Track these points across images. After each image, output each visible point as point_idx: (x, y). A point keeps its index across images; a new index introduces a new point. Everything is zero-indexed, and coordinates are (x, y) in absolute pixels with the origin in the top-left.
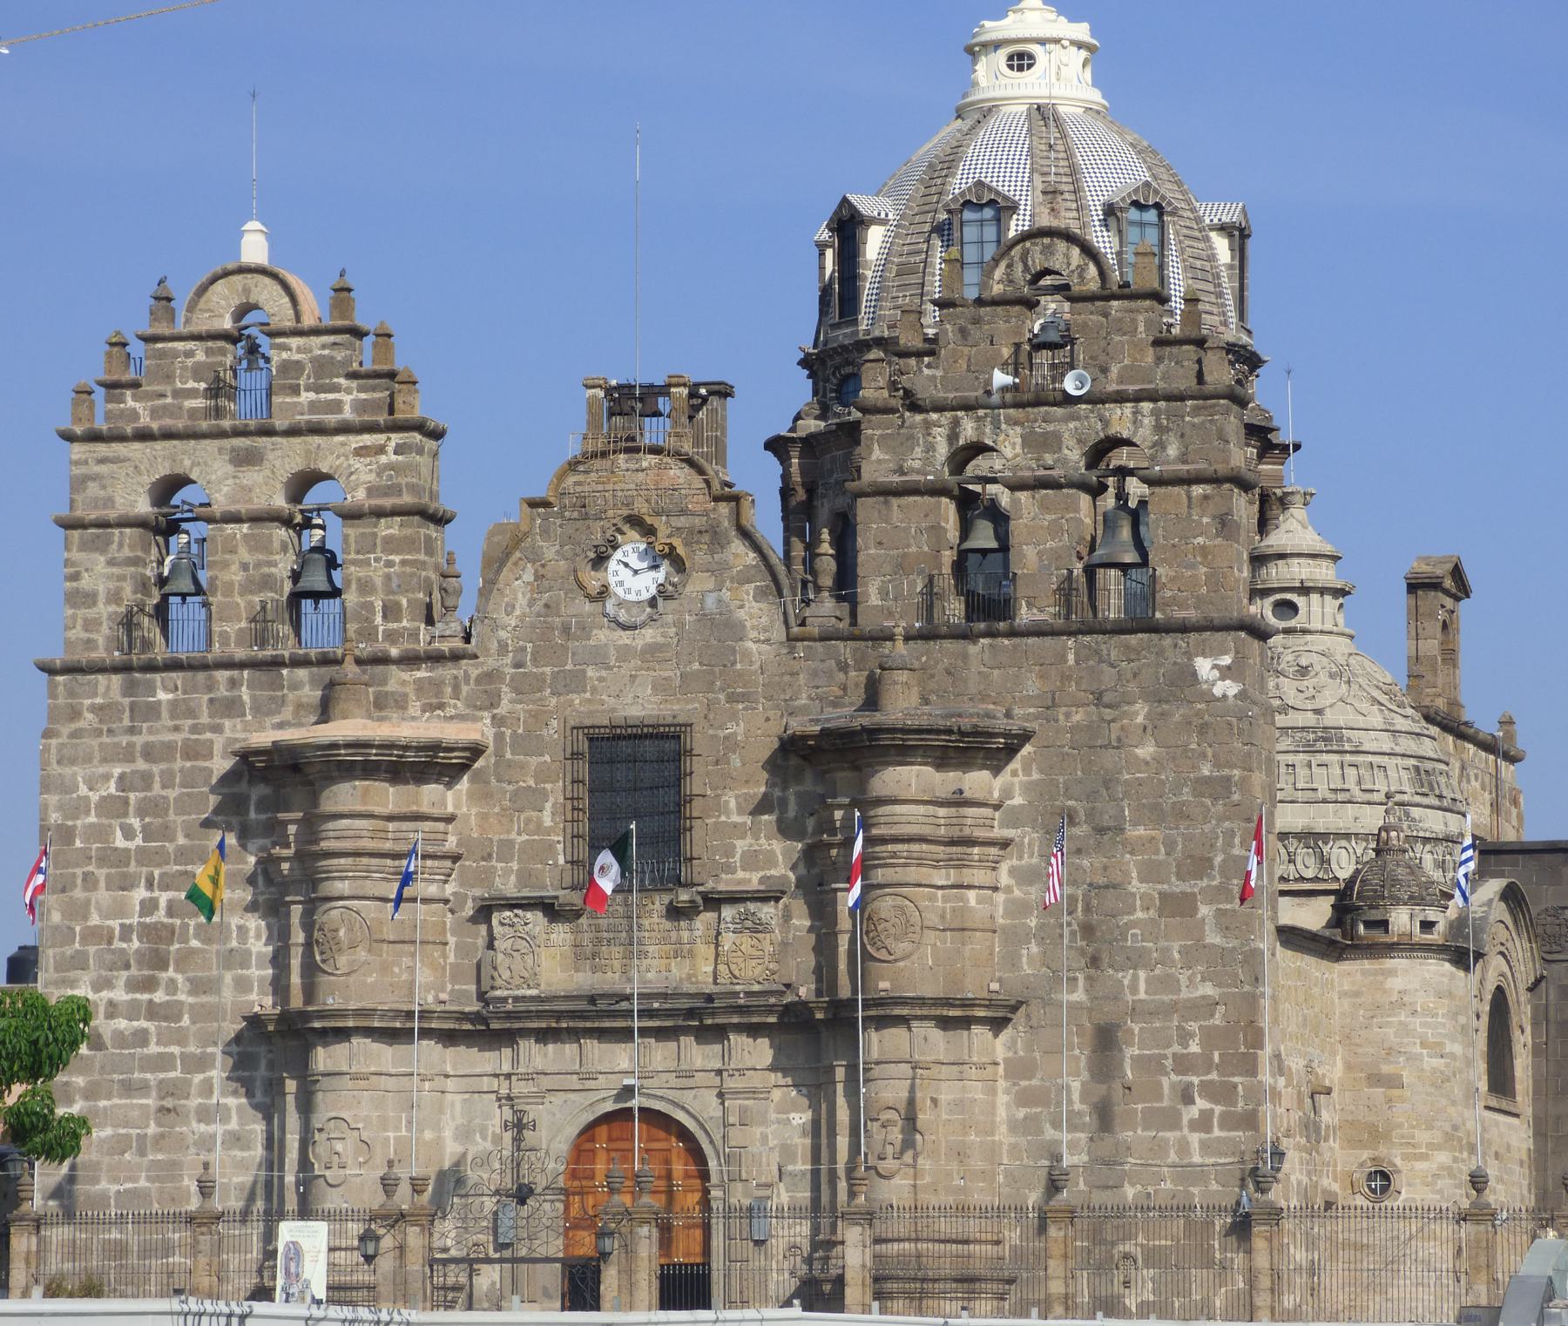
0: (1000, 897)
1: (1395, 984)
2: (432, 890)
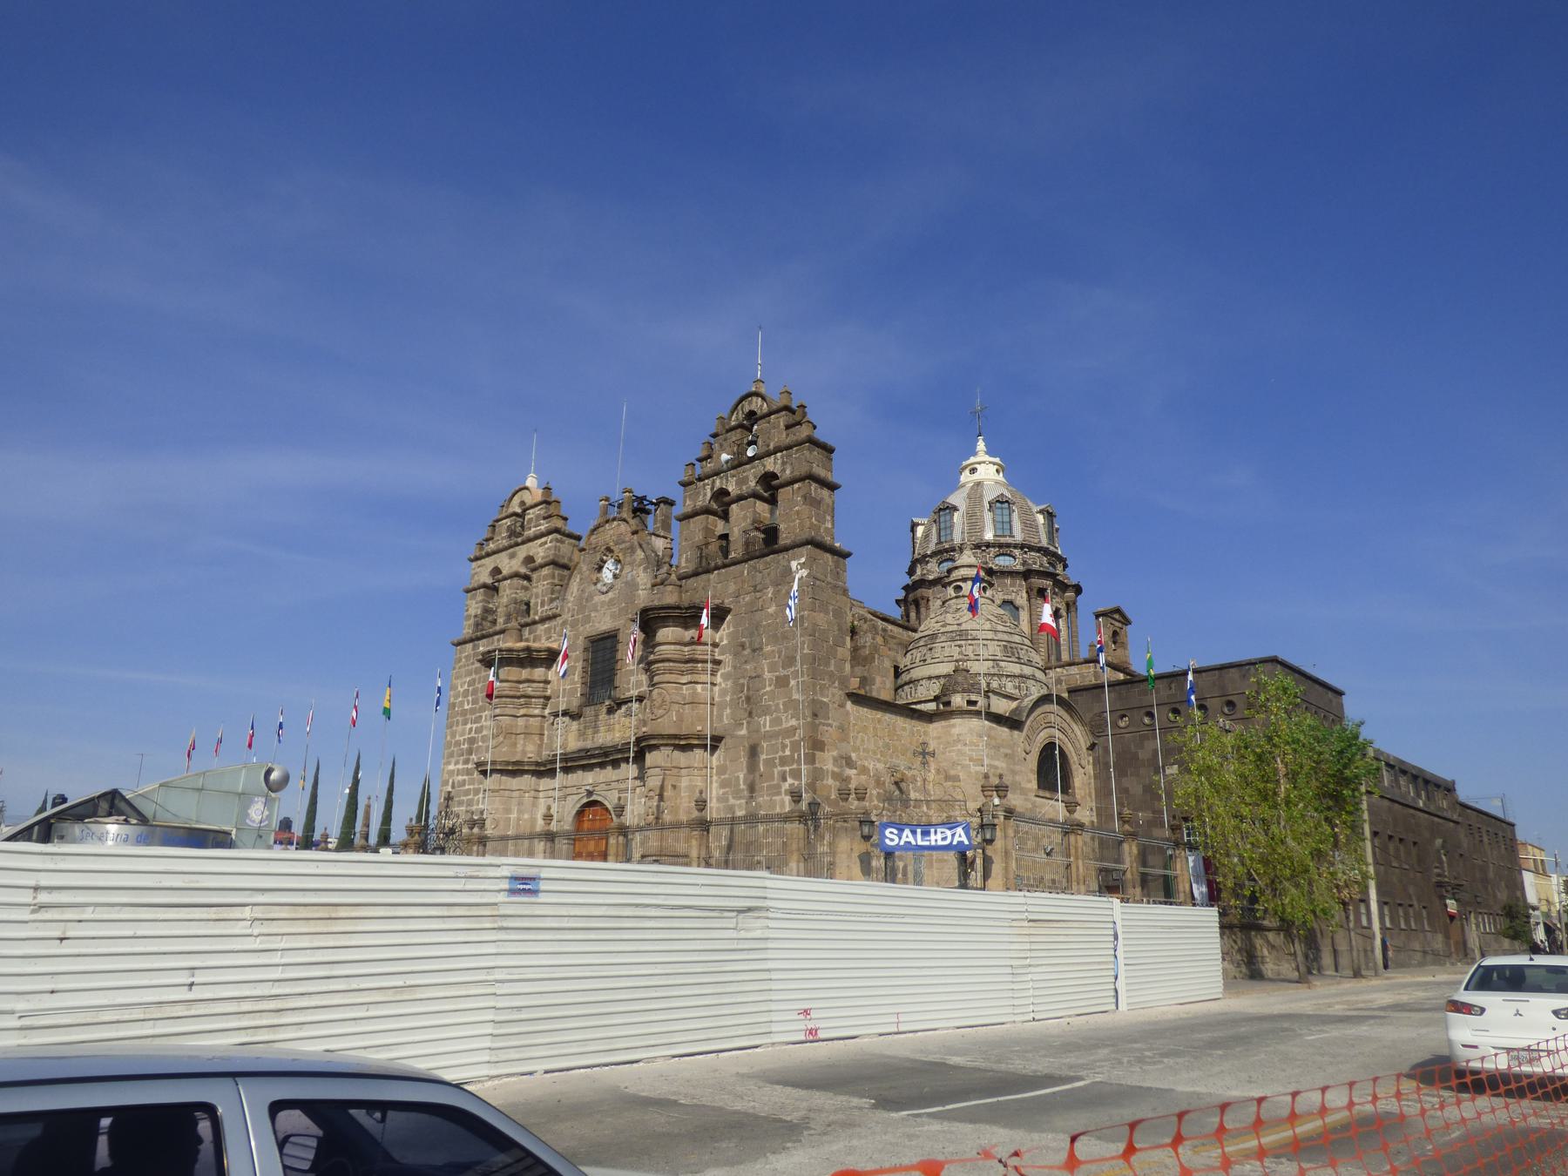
0: (716, 689)
1: (955, 731)
2: (537, 712)
